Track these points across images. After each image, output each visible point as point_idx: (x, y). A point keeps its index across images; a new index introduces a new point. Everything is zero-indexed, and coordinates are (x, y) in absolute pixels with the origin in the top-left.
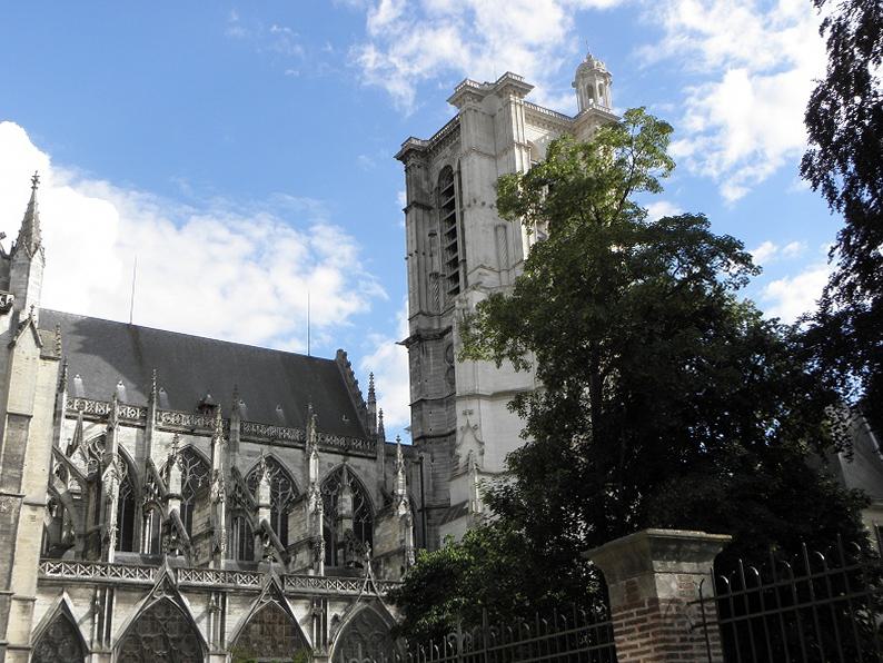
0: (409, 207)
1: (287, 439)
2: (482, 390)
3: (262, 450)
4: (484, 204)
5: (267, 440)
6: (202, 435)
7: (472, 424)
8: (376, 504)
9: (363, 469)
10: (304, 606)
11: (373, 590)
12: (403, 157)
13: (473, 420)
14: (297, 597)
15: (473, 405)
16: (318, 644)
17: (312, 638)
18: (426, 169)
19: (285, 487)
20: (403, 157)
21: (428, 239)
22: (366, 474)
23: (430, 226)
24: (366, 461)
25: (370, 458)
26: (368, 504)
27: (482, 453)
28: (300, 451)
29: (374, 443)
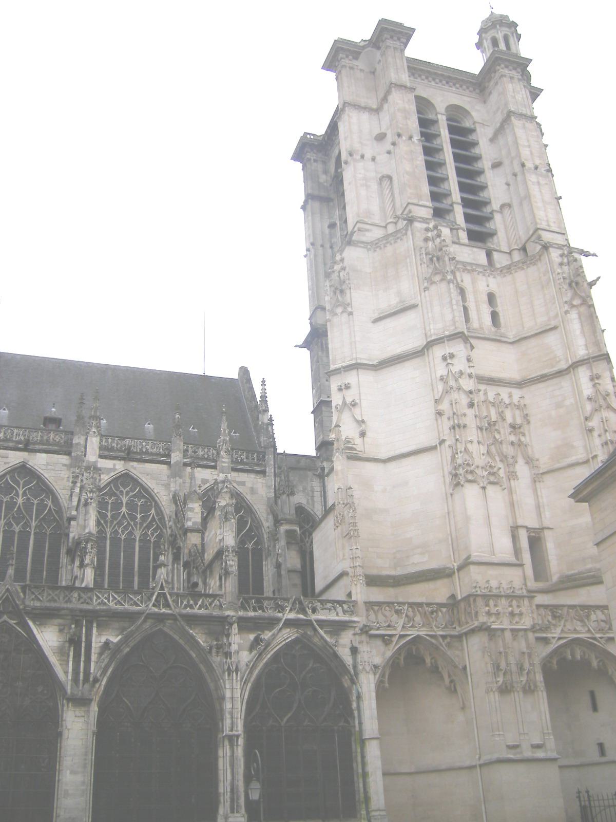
0: (306, 202)
1: (147, 453)
2: (363, 358)
3: (114, 465)
4: (362, 157)
5: (122, 454)
6: (40, 451)
7: (349, 400)
8: (266, 524)
9: (249, 485)
10: (56, 629)
11: (167, 605)
12: (298, 156)
13: (350, 396)
14: (44, 616)
15: (351, 378)
16: (75, 680)
17: (66, 673)
18: (324, 163)
19: (146, 509)
20: (298, 156)
21: (327, 231)
22: (253, 491)
23: (330, 218)
24: (252, 476)
25: (257, 472)
26: (257, 524)
27: (363, 434)
28: (165, 467)
29: (262, 457)
